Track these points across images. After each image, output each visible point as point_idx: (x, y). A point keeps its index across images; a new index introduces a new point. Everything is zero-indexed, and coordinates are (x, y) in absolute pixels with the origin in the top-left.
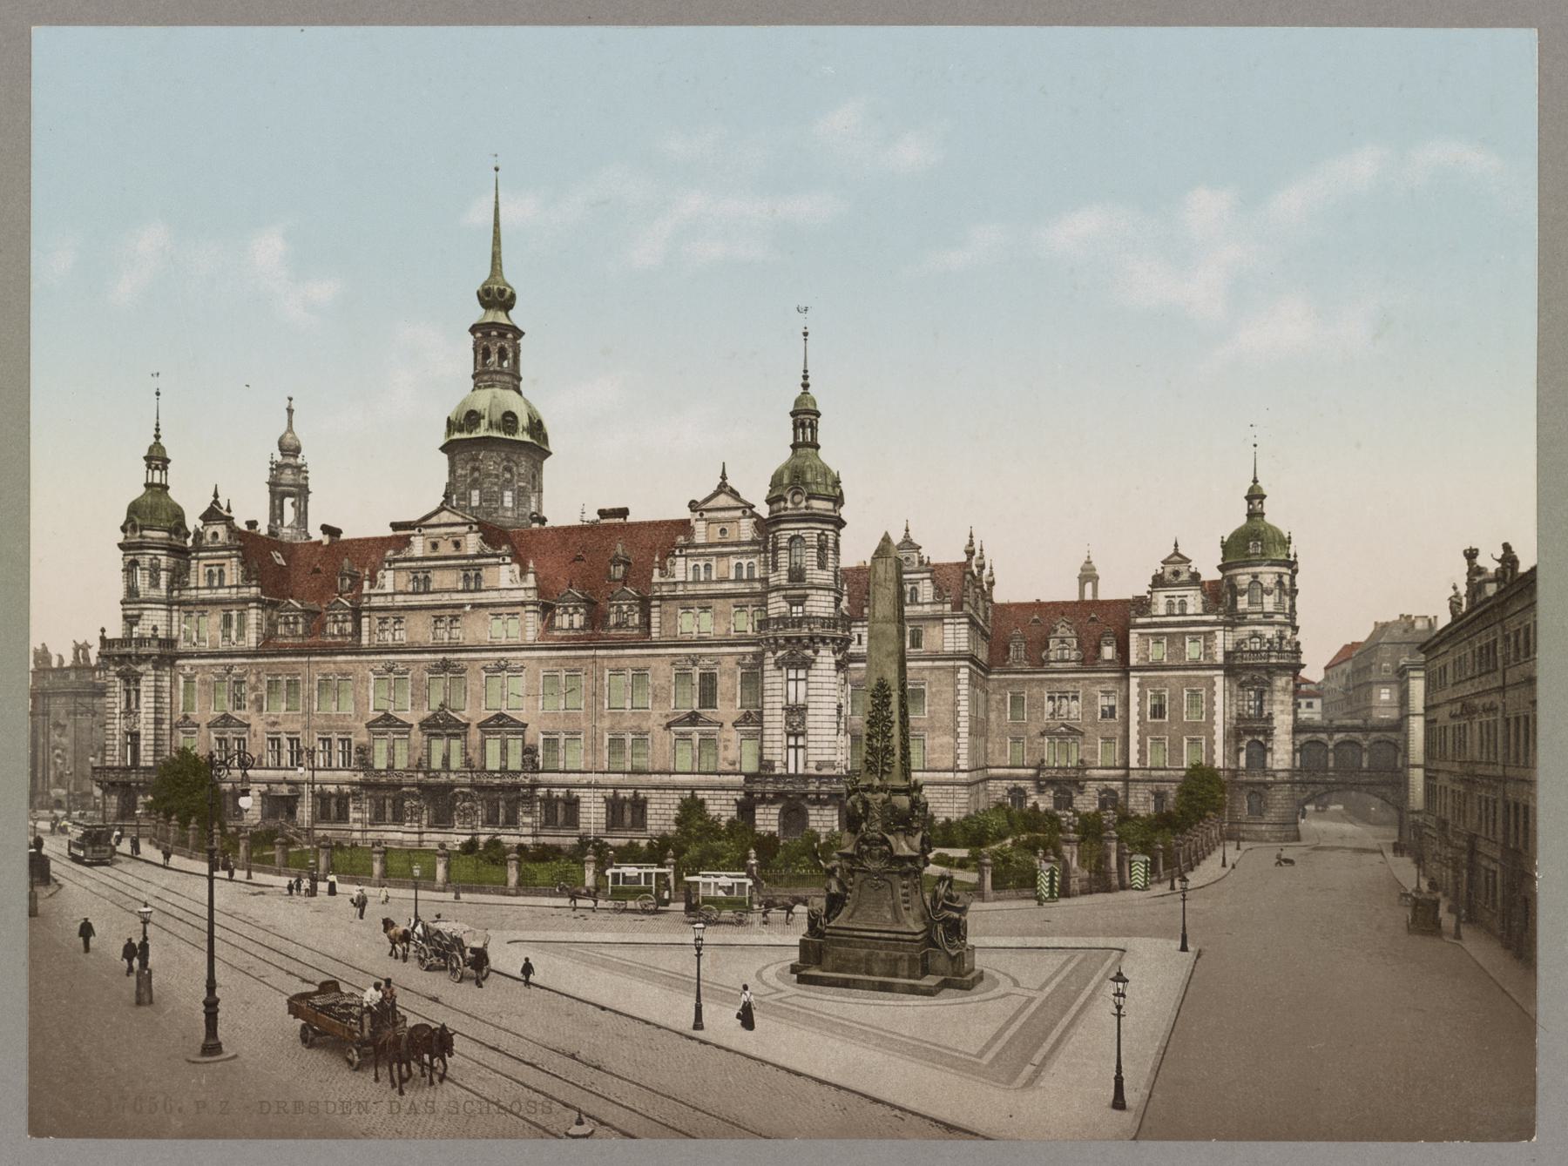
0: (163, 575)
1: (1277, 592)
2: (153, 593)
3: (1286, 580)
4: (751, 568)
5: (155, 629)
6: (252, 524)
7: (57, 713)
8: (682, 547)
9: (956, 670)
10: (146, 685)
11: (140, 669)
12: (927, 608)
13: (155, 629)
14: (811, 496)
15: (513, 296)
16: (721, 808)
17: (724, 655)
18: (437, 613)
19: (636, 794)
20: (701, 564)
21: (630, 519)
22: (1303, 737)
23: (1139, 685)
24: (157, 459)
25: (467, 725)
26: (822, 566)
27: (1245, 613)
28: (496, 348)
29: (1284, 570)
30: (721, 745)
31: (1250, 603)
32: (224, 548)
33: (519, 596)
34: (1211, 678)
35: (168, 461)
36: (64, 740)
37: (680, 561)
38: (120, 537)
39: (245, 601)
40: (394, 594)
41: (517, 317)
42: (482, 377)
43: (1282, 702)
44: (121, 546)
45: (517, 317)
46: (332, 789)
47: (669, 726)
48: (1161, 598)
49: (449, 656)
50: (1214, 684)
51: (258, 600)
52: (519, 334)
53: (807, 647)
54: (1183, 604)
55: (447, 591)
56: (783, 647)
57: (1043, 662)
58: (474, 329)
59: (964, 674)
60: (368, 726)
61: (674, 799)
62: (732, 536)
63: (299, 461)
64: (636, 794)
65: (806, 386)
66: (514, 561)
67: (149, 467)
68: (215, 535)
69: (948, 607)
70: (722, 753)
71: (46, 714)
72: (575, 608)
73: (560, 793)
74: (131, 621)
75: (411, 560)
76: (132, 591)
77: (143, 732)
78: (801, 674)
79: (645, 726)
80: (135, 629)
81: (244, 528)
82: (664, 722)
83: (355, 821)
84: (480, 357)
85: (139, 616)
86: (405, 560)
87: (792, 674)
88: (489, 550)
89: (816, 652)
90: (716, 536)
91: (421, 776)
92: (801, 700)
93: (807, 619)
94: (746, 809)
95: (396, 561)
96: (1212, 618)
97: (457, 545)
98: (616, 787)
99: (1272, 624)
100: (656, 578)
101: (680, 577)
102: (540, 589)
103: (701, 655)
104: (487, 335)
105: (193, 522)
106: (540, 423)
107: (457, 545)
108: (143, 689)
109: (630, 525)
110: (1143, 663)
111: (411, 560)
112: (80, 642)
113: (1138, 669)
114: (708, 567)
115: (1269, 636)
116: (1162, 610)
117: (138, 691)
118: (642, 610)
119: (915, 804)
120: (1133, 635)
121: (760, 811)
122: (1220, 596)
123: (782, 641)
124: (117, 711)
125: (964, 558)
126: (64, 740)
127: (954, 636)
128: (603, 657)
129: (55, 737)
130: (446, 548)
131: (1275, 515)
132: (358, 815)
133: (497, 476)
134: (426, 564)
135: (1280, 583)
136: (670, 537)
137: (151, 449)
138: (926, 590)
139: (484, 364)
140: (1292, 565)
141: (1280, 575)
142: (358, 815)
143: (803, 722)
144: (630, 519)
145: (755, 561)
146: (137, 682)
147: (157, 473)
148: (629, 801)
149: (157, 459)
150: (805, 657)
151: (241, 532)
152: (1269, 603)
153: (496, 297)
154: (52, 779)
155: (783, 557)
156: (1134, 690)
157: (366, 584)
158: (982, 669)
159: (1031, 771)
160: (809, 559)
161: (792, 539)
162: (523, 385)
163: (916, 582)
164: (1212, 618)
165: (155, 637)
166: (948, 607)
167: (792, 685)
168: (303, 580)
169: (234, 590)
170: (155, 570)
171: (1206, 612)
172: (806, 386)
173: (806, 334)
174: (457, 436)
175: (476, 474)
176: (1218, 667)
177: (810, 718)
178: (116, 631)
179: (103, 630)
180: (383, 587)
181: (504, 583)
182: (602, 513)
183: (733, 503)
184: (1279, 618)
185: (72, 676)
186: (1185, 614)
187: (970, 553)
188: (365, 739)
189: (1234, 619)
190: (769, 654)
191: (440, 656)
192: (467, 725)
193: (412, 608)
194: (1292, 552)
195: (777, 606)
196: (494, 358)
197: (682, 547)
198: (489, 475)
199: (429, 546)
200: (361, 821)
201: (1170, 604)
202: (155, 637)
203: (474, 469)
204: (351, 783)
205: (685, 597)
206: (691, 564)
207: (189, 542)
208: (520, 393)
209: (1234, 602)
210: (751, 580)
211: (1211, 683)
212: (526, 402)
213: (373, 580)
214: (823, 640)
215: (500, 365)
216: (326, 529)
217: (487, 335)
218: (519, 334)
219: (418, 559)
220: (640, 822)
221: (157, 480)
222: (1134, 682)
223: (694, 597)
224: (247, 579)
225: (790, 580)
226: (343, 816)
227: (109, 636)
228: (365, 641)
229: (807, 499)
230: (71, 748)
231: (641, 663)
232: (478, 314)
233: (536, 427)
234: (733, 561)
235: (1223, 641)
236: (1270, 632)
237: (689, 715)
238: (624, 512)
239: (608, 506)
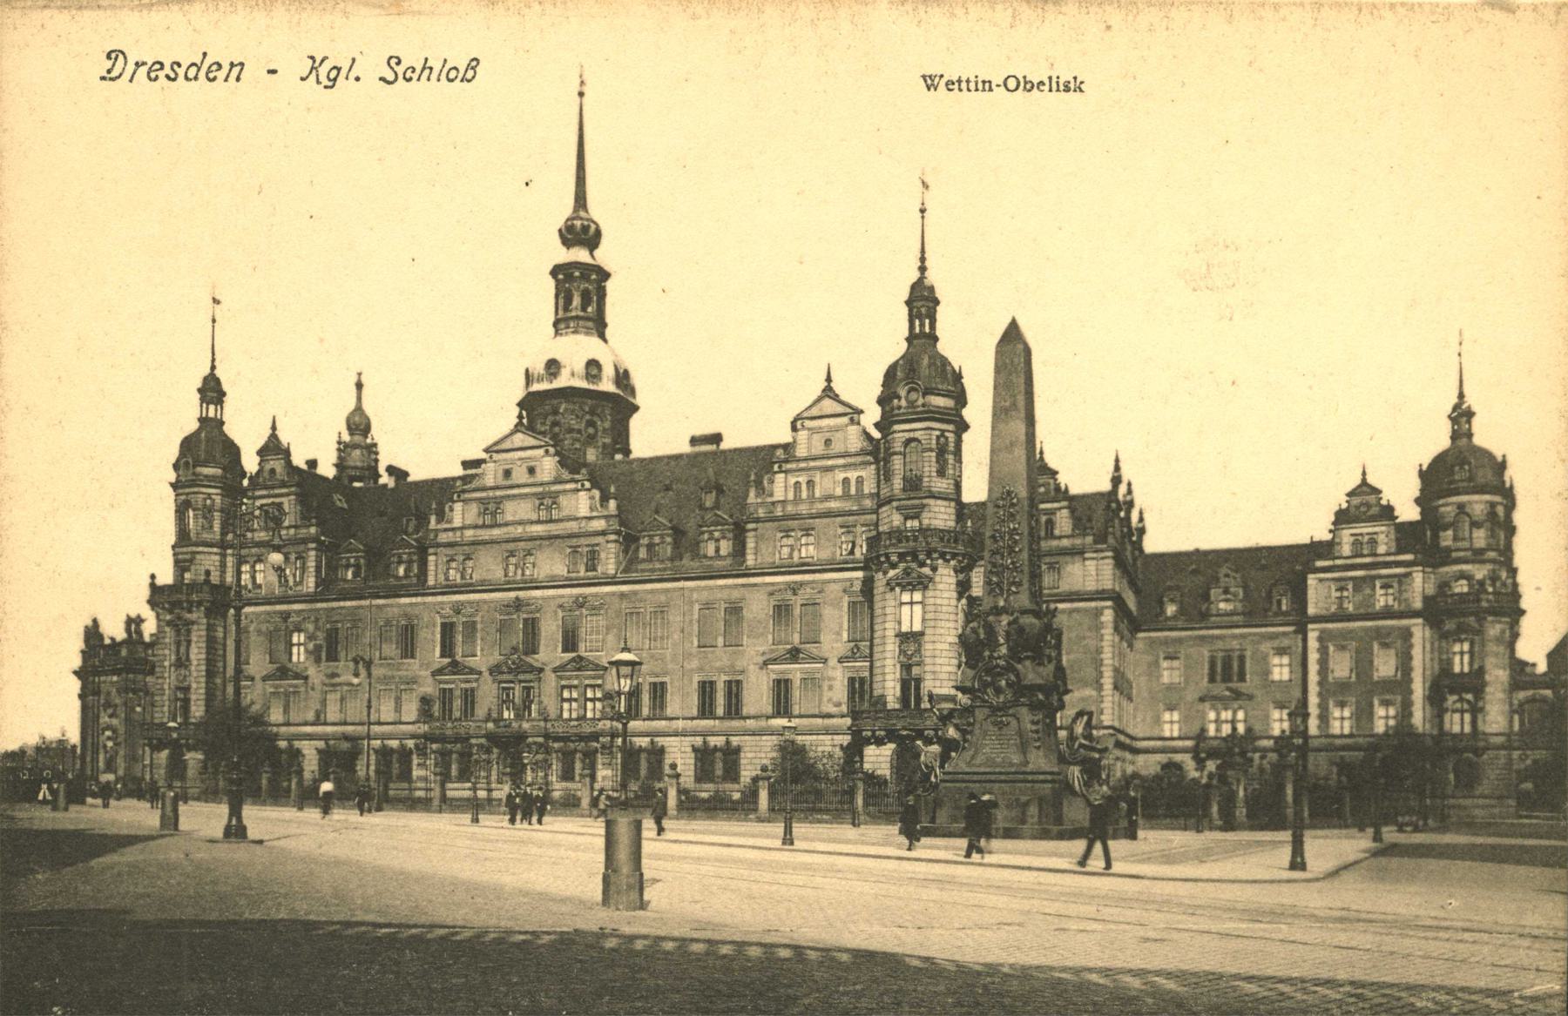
0: (217, 514)
1: (1488, 524)
2: (206, 536)
3: (1500, 510)
4: (860, 481)
5: (208, 573)
6: (312, 464)
7: (109, 693)
8: (781, 462)
9: (1098, 613)
10: (198, 636)
11: (193, 616)
12: (1065, 542)
14: (927, 392)
15: (598, 233)
16: (826, 746)
17: (829, 581)
18: (511, 546)
19: (728, 742)
20: (803, 479)
21: (725, 445)
22: (1522, 695)
23: (1320, 639)
24: (212, 390)
25: (541, 670)
26: (941, 473)
27: (1448, 550)
28: (581, 294)
29: (1497, 499)
30: (825, 685)
31: (1455, 539)
32: (283, 485)
33: (599, 525)
36: (115, 721)
37: (780, 477)
38: (172, 477)
39: (304, 541)
40: (462, 528)
41: (604, 255)
42: (561, 324)
43: (1497, 655)
44: (175, 486)
45: (604, 255)
46: (394, 744)
47: (765, 663)
48: (1346, 536)
49: (521, 594)
50: (1411, 635)
51: (316, 540)
52: (605, 275)
54: (1373, 542)
55: (520, 523)
56: (894, 566)
57: (1205, 616)
58: (555, 272)
59: (1108, 616)
60: (434, 674)
61: (770, 742)
62: (837, 447)
63: (369, 441)
64: (728, 742)
65: (923, 269)
66: (593, 486)
67: (202, 400)
68: (273, 471)
69: (1089, 539)
70: (827, 694)
71: (97, 693)
72: (662, 536)
73: (643, 742)
74: (181, 566)
75: (484, 489)
76: (183, 537)
77: (194, 686)
78: (917, 596)
79: (739, 665)
80: (187, 575)
81: (304, 467)
82: (761, 659)
83: (420, 778)
84: (561, 302)
85: (191, 561)
86: (475, 490)
87: (906, 597)
88: (566, 475)
89: (934, 569)
90: (818, 449)
91: (490, 725)
92: (917, 627)
93: (924, 531)
94: (854, 751)
95: (464, 491)
96: (1409, 557)
97: (531, 471)
98: (704, 734)
99: (1483, 562)
100: (752, 498)
101: (779, 494)
102: (621, 516)
103: (802, 584)
104: (569, 278)
105: (250, 463)
106: (626, 372)
107: (531, 471)
108: (194, 639)
109: (724, 452)
110: (1324, 612)
111: (484, 489)
112: (133, 615)
113: (1318, 619)
114: (810, 483)
115: (1479, 576)
116: (1346, 550)
117: (189, 642)
118: (735, 538)
119: (1048, 628)
120: (1312, 580)
121: (870, 751)
122: (1419, 541)
123: (894, 558)
124: (167, 664)
125: (1106, 486)
126: (115, 721)
127: (1093, 572)
128: (692, 590)
129: (105, 719)
130: (520, 475)
131: (1484, 435)
132: (422, 773)
133: (579, 431)
134: (498, 493)
135: (1492, 514)
136: (766, 460)
137: (205, 379)
138: (1063, 523)
139: (566, 309)
140: (1509, 495)
141: (1493, 505)
142: (422, 773)
143: (918, 651)
144: (725, 445)
145: (863, 473)
146: (189, 632)
147: (212, 407)
148: (720, 750)
149: (212, 390)
151: (297, 469)
152: (1480, 538)
153: (580, 233)
154: (101, 764)
155: (897, 462)
156: (1313, 644)
157: (433, 519)
158: (1129, 624)
159: (1189, 743)
160: (929, 466)
161: (908, 442)
162: (608, 332)
163: (1052, 512)
164: (1409, 557)
165: (207, 582)
166: (1089, 539)
167: (906, 609)
168: (363, 519)
169: (292, 531)
170: (207, 512)
171: (1400, 551)
172: (923, 269)
173: (923, 211)
174: (536, 387)
175: (557, 429)
176: (1415, 614)
177: (928, 646)
178: (166, 577)
179: (153, 577)
180: (450, 522)
181: (584, 510)
182: (694, 441)
183: (840, 409)
184: (1492, 554)
185: (124, 652)
186: (1375, 555)
187: (1116, 481)
189: (1434, 557)
190: (880, 575)
191: (512, 594)
192: (541, 670)
193: (484, 543)
194: (1507, 478)
195: (892, 519)
196: (576, 301)
197: (781, 462)
198: (571, 431)
199: (500, 473)
200: (425, 779)
201: (1357, 544)
202: (207, 582)
203: (555, 424)
204: (413, 736)
205: (786, 518)
206: (792, 480)
207: (246, 482)
208: (605, 341)
209: (1436, 537)
210: (860, 495)
211: (1407, 634)
212: (613, 351)
213: (441, 516)
214: (942, 555)
215: (584, 309)
216: (391, 470)
217: (569, 278)
218: (605, 275)
219: (492, 488)
220: (732, 773)
221: (211, 414)
222: (1312, 636)
223: (793, 517)
224: (305, 518)
225: (904, 490)
226: (406, 775)
227: (160, 581)
228: (431, 582)
229: (924, 395)
230: (122, 730)
231: (736, 594)
232: (564, 255)
233: (623, 378)
234: (841, 476)
235: (1420, 584)
236: (1480, 572)
237: (789, 651)
238: (716, 438)
239: (699, 432)
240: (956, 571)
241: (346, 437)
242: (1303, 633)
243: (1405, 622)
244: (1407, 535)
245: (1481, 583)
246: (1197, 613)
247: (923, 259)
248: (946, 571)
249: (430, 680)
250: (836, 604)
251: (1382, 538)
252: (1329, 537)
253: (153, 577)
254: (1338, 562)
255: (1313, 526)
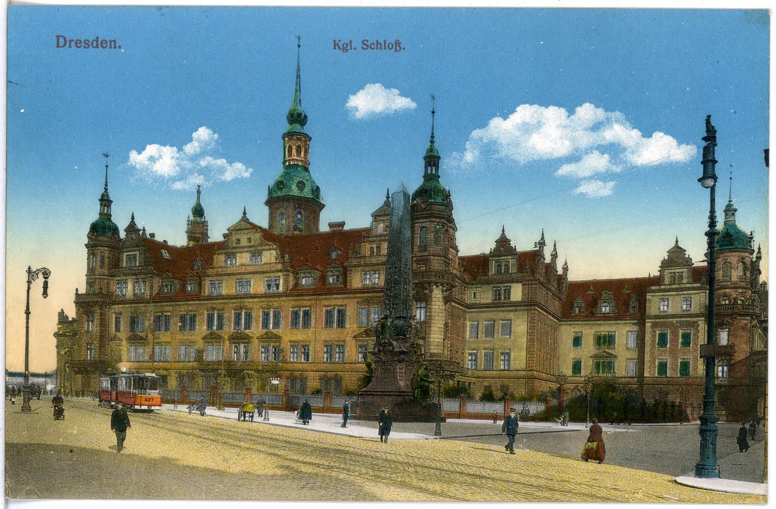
13: (101, 289)
15: (306, 117)
20: (375, 246)
34: (697, 322)
35: (111, 202)
41: (307, 129)
45: (307, 129)
53: (426, 289)
54: (681, 277)
67: (101, 205)
78: (423, 305)
105: (123, 235)
106: (318, 188)
113: (650, 317)
139: (290, 155)
144: (346, 228)
150: (425, 294)
179: (77, 290)
188: (202, 346)
214: (436, 284)
222: (648, 325)
227: (80, 292)
233: (316, 191)
238: (342, 224)
240: (443, 292)
241: (192, 218)
242: (642, 325)
243: (695, 319)
244: (697, 274)
245: (735, 299)
246: (591, 314)
247: (432, 137)
248: (438, 292)
249: (201, 341)
250: (286, 317)
251: (685, 275)
252: (658, 274)
253: (77, 290)
254: (663, 287)
255: (652, 270)
